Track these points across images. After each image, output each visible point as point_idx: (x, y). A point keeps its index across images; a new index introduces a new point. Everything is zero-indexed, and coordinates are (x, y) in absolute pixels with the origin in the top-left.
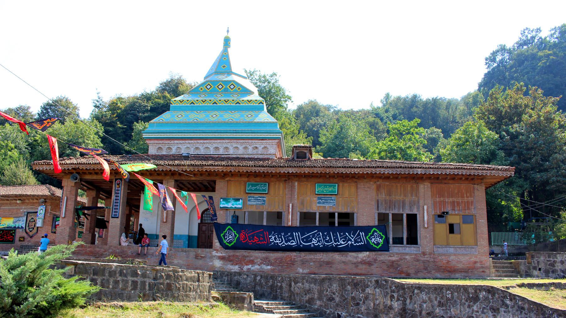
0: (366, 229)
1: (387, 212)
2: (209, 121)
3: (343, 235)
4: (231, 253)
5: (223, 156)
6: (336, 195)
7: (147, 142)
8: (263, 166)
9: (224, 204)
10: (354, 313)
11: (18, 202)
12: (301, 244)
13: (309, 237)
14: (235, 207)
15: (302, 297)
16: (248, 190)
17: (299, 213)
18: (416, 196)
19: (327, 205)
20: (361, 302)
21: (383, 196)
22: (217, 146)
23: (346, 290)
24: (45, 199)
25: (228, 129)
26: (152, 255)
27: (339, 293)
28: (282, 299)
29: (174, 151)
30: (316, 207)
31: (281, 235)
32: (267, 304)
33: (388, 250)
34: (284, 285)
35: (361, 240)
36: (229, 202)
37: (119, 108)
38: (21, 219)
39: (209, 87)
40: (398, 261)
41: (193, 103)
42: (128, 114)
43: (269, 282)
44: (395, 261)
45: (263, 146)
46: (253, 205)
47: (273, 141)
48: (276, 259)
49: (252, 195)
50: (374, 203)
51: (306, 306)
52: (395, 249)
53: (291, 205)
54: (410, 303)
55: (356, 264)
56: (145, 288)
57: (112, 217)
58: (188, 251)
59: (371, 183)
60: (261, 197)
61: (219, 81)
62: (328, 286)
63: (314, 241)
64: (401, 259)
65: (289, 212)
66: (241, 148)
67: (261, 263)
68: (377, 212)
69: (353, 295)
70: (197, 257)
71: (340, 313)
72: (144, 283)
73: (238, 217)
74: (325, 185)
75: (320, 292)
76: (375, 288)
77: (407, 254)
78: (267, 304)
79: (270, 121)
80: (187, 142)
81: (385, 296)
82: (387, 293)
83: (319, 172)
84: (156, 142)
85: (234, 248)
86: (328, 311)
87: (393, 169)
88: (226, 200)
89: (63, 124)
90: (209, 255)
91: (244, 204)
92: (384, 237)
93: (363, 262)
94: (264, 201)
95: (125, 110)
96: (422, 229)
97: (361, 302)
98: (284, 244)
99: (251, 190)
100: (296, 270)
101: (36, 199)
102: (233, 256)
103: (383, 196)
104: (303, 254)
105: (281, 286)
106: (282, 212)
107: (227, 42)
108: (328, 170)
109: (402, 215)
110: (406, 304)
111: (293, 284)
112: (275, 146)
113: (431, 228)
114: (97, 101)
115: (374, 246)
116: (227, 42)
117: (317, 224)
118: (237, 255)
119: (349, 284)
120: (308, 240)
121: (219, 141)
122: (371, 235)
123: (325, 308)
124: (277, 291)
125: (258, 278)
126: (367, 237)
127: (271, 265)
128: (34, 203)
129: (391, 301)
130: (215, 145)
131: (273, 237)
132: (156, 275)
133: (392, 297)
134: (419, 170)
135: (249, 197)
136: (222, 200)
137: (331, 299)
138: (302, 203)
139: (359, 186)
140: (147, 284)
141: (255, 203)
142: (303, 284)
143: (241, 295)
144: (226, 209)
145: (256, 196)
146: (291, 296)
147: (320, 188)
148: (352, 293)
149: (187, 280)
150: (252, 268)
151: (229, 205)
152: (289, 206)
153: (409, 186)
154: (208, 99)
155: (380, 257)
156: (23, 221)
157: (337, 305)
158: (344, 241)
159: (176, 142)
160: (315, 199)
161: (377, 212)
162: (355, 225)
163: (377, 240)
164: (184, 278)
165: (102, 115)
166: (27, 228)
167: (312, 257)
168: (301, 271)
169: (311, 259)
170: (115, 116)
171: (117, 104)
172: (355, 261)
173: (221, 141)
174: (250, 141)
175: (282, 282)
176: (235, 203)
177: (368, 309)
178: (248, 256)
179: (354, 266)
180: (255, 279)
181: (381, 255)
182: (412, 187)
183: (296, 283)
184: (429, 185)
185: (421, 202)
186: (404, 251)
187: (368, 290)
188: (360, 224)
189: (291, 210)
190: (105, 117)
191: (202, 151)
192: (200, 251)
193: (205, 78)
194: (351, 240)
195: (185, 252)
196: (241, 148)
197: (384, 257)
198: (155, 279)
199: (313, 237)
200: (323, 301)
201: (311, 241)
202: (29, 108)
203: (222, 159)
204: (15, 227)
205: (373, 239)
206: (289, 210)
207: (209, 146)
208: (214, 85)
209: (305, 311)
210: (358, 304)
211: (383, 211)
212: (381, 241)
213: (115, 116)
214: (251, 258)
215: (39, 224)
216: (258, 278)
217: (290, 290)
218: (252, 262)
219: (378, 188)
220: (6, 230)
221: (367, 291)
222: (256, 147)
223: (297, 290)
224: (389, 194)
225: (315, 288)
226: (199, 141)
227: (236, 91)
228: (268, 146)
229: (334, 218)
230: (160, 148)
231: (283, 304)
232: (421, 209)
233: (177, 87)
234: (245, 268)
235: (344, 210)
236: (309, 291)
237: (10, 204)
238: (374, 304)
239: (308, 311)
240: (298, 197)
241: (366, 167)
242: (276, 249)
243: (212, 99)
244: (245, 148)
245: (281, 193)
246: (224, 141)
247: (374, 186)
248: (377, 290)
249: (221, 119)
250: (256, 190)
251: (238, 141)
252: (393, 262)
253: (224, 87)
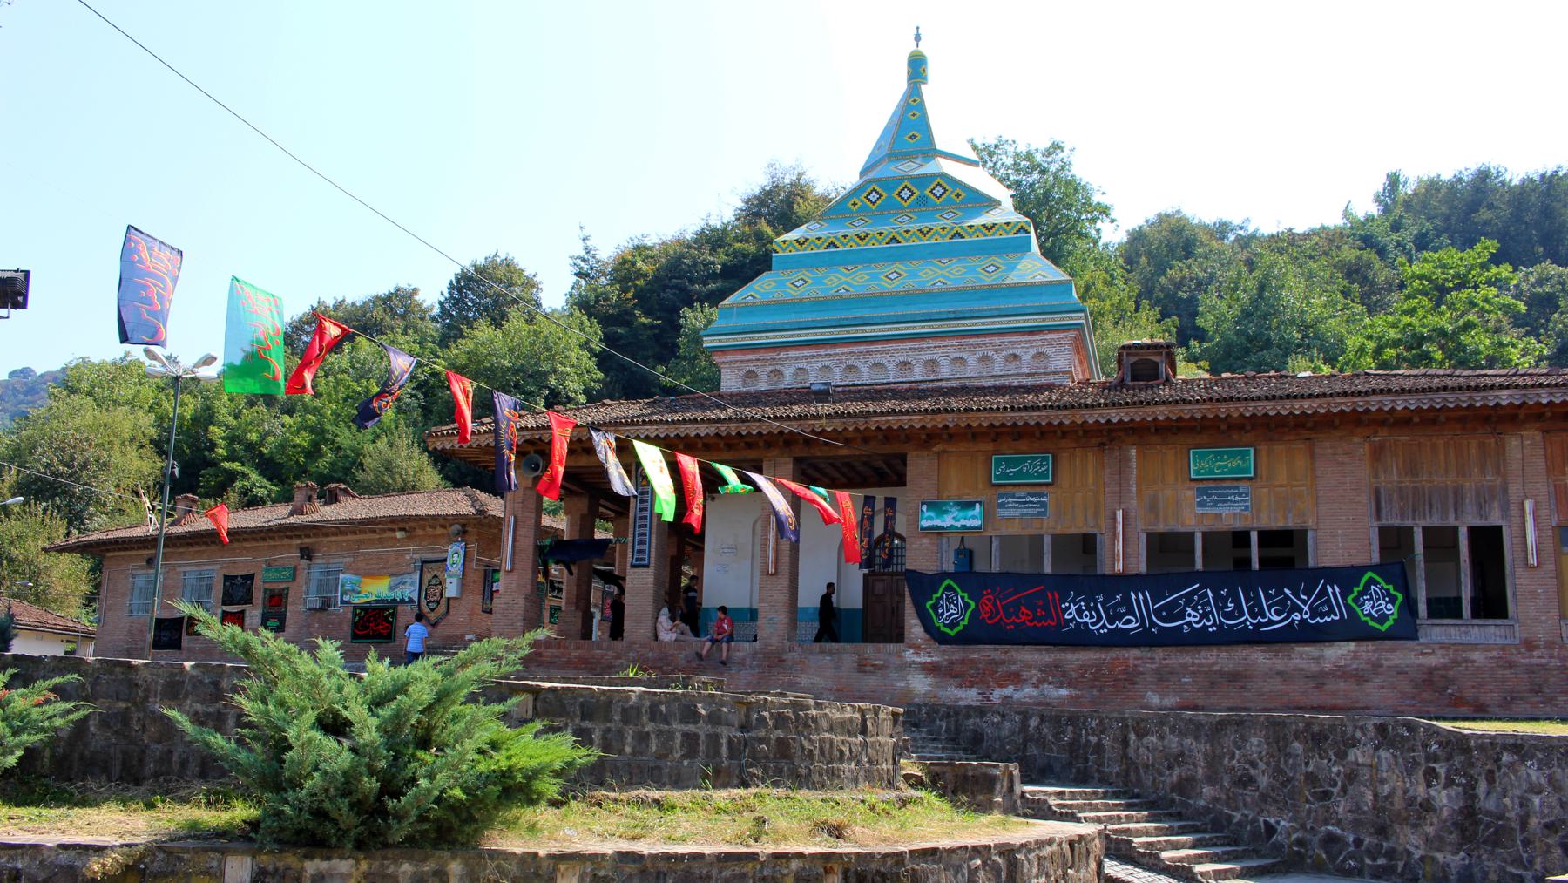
0: (1346, 577)
1: (1408, 523)
2: (879, 290)
3: (1277, 595)
4: (956, 653)
5: (923, 386)
6: (1250, 479)
7: (716, 359)
8: (1035, 408)
9: (930, 518)
10: (1315, 820)
11: (399, 535)
12: (1153, 624)
13: (1175, 602)
14: (964, 527)
15: (1161, 774)
16: (997, 477)
17: (1144, 537)
18: (1498, 473)
19: (1225, 511)
20: (1335, 790)
21: (1392, 477)
22: (905, 358)
23: (1289, 755)
24: (463, 526)
25: (934, 309)
26: (742, 663)
27: (1267, 764)
28: (1103, 781)
29: (788, 380)
30: (1193, 515)
31: (1096, 603)
32: (1060, 795)
33: (1414, 636)
34: (1107, 742)
35: (1331, 607)
36: (946, 512)
37: (641, 274)
38: (407, 578)
39: (874, 197)
40: (1445, 667)
41: (832, 244)
42: (665, 287)
43: (1064, 732)
44: (1436, 668)
45: (1033, 352)
46: (1014, 518)
47: (1062, 335)
48: (1083, 668)
49: (1009, 490)
50: (1365, 498)
51: (1173, 801)
52: (1437, 633)
53: (1119, 514)
54: (1488, 793)
55: (1319, 679)
56: (717, 753)
57: (633, 566)
58: (838, 652)
59: (1356, 439)
60: (1033, 495)
61: (903, 178)
62: (1235, 743)
63: (1192, 617)
64: (1456, 662)
65: (1115, 535)
66: (971, 359)
67: (1042, 681)
68: (1376, 524)
69: (1310, 769)
70: (861, 667)
71: (1272, 821)
72: (714, 739)
73: (971, 552)
74: (1216, 454)
75: (1213, 761)
76: (1377, 748)
77: (1474, 647)
78: (1060, 795)
79: (1050, 278)
80: (822, 352)
81: (1410, 772)
82: (1416, 763)
83: (1198, 416)
84: (740, 357)
85: (965, 639)
86: (1237, 816)
87: (1422, 396)
88: (936, 506)
89: (498, 325)
90: (895, 660)
91: (988, 516)
92: (1400, 597)
93: (1341, 673)
94: (1043, 505)
95: (656, 278)
96: (1519, 571)
97: (1335, 790)
98: (1104, 626)
99: (1006, 476)
100: (1143, 697)
101: (443, 526)
102: (963, 662)
103: (1392, 477)
104: (1159, 653)
105: (1099, 746)
106: (1094, 536)
107: (917, 67)
108: (1223, 410)
109: (1455, 530)
110: (1475, 796)
111: (1133, 736)
112: (1068, 350)
113: (1550, 566)
114: (584, 260)
115: (1372, 624)
116: (917, 67)
117: (1199, 565)
118: (973, 661)
119: (1297, 737)
120: (1173, 612)
121: (909, 345)
122: (1361, 593)
123: (1229, 807)
124: (1087, 760)
125: (1034, 722)
126: (1350, 600)
127: (1070, 684)
128: (435, 536)
129: (1429, 785)
130: (900, 357)
131: (1073, 608)
132: (747, 716)
133: (1431, 775)
134: (1505, 393)
135: (1001, 496)
136: (924, 508)
137: (1245, 781)
138: (1153, 507)
139: (1317, 450)
140: (724, 741)
141: (1018, 512)
142: (1162, 738)
143: (984, 770)
144: (938, 532)
145: (1021, 492)
146: (1127, 774)
147: (1200, 463)
148: (1307, 764)
149: (831, 730)
150: (1016, 696)
151: (946, 521)
152: (1114, 518)
153: (1474, 443)
154: (873, 230)
155: (1389, 655)
156: (412, 584)
157: (1264, 798)
158: (1278, 613)
159: (792, 353)
160: (1189, 493)
161: (1376, 524)
162: (1311, 563)
163: (1378, 606)
164: (824, 724)
165: (597, 297)
166: (424, 602)
167: (1187, 659)
168: (1155, 700)
169: (1185, 666)
170: (629, 295)
171: (633, 264)
172: (1314, 668)
173: (916, 344)
174: (996, 340)
175: (1102, 732)
176: (962, 514)
177: (1357, 809)
178: (1003, 662)
179: (1311, 684)
180: (1024, 725)
181: (1393, 650)
182: (1482, 446)
183: (1140, 736)
184: (1538, 437)
185: (1514, 490)
186: (1465, 639)
187: (1356, 755)
188: (1327, 562)
189: (1120, 528)
190: (606, 299)
191: (866, 374)
192: (869, 649)
193: (862, 174)
194: (1300, 610)
195: (831, 653)
196: (971, 359)
197: (1403, 656)
198: (744, 727)
199: (1187, 604)
200: (1222, 787)
201: (1181, 616)
202: (415, 291)
203: (922, 394)
204: (394, 600)
205: (1368, 605)
206: (1115, 528)
207: (883, 361)
208: (889, 189)
209: (1170, 815)
210: (1326, 795)
211: (1396, 522)
212: (1392, 610)
213: (629, 295)
214: (1014, 668)
215: (451, 590)
216: (1034, 722)
217: (1125, 756)
218: (1016, 679)
219: (1377, 453)
220: (375, 609)
221: (1351, 758)
222: (1015, 356)
223: (1145, 756)
224: (1412, 469)
225: (1198, 749)
226: (855, 349)
227: (949, 202)
228: (1048, 350)
229: (1248, 545)
230: (750, 374)
231: (1105, 796)
232: (1514, 510)
233: (790, 205)
234: (997, 695)
235: (1277, 523)
236: (1179, 758)
237: (381, 542)
238: (1376, 796)
239: (1179, 814)
240: (1139, 491)
241: (1338, 395)
242: (1081, 639)
243: (885, 229)
244: (985, 359)
245: (1090, 480)
246: (925, 344)
247: (1364, 450)
248: (1384, 754)
249: (911, 284)
250: (1018, 475)
251: (963, 342)
252: (1431, 671)
253: (917, 193)
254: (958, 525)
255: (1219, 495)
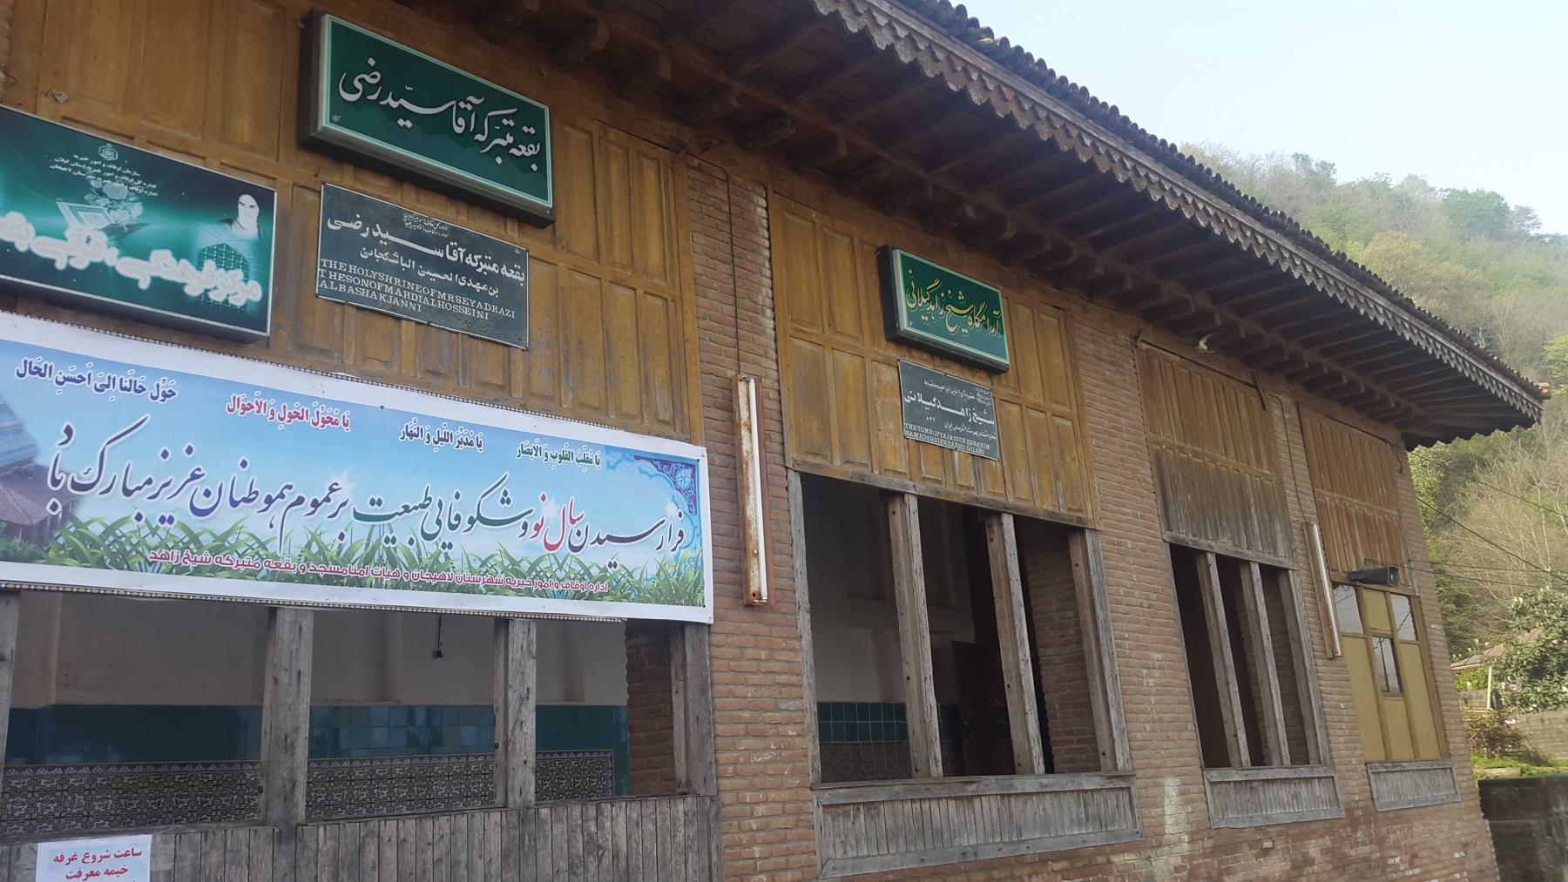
17: (795, 483)
36: (75, 190)
49: (376, 190)
60: (475, 245)
94: (512, 294)
135: (341, 206)
176: (161, 225)
235: (1044, 505)
254: (141, 272)
255: (946, 400)
